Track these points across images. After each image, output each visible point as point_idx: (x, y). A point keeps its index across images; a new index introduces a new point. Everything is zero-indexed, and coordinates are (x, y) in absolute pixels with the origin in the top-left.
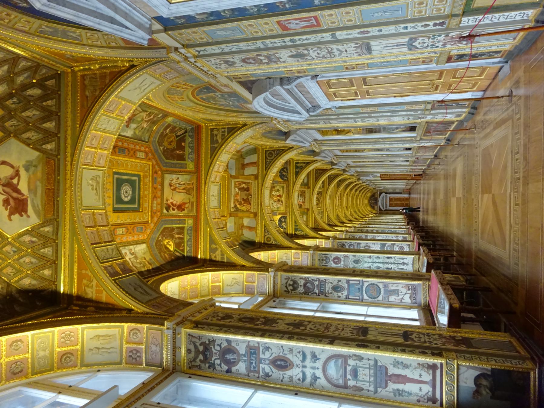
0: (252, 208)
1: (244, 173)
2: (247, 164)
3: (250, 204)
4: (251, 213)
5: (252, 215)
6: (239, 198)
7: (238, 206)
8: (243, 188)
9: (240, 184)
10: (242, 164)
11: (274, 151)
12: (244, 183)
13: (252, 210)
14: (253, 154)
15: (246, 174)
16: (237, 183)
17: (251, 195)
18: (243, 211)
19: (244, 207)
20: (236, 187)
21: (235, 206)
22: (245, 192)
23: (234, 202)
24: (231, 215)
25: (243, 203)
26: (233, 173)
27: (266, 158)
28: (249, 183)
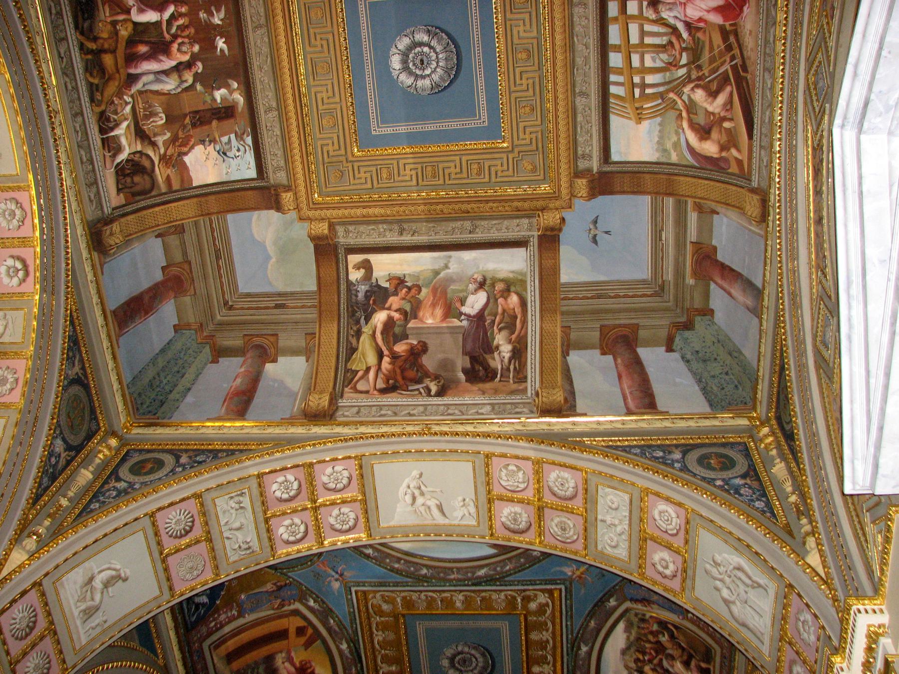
0: (363, 401)
1: (582, 346)
2: (636, 367)
3: (383, 391)
4: (334, 399)
5: (325, 401)
6: (431, 318)
7: (380, 317)
8: (490, 348)
9: (510, 326)
10: (635, 328)
11: (752, 473)
12: (519, 353)
13: (349, 400)
14: (705, 391)
15: (574, 358)
16: (514, 299)
17: (441, 393)
18: (352, 351)
19: (372, 359)
20: (492, 299)
21: (378, 295)
22: (461, 362)
23: (399, 282)
24: (326, 251)
25: (400, 348)
26: (574, 268)
27: (686, 449)
28: (521, 377)
